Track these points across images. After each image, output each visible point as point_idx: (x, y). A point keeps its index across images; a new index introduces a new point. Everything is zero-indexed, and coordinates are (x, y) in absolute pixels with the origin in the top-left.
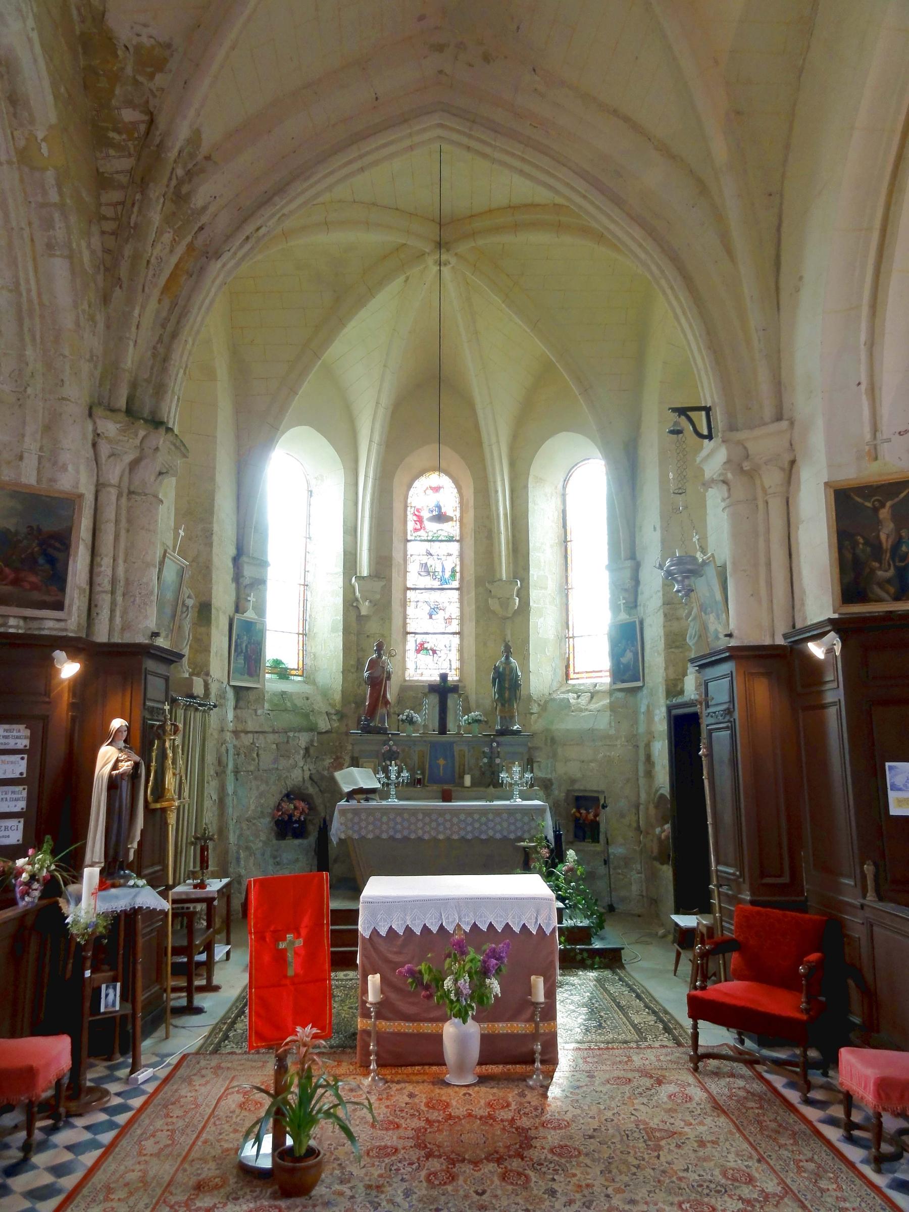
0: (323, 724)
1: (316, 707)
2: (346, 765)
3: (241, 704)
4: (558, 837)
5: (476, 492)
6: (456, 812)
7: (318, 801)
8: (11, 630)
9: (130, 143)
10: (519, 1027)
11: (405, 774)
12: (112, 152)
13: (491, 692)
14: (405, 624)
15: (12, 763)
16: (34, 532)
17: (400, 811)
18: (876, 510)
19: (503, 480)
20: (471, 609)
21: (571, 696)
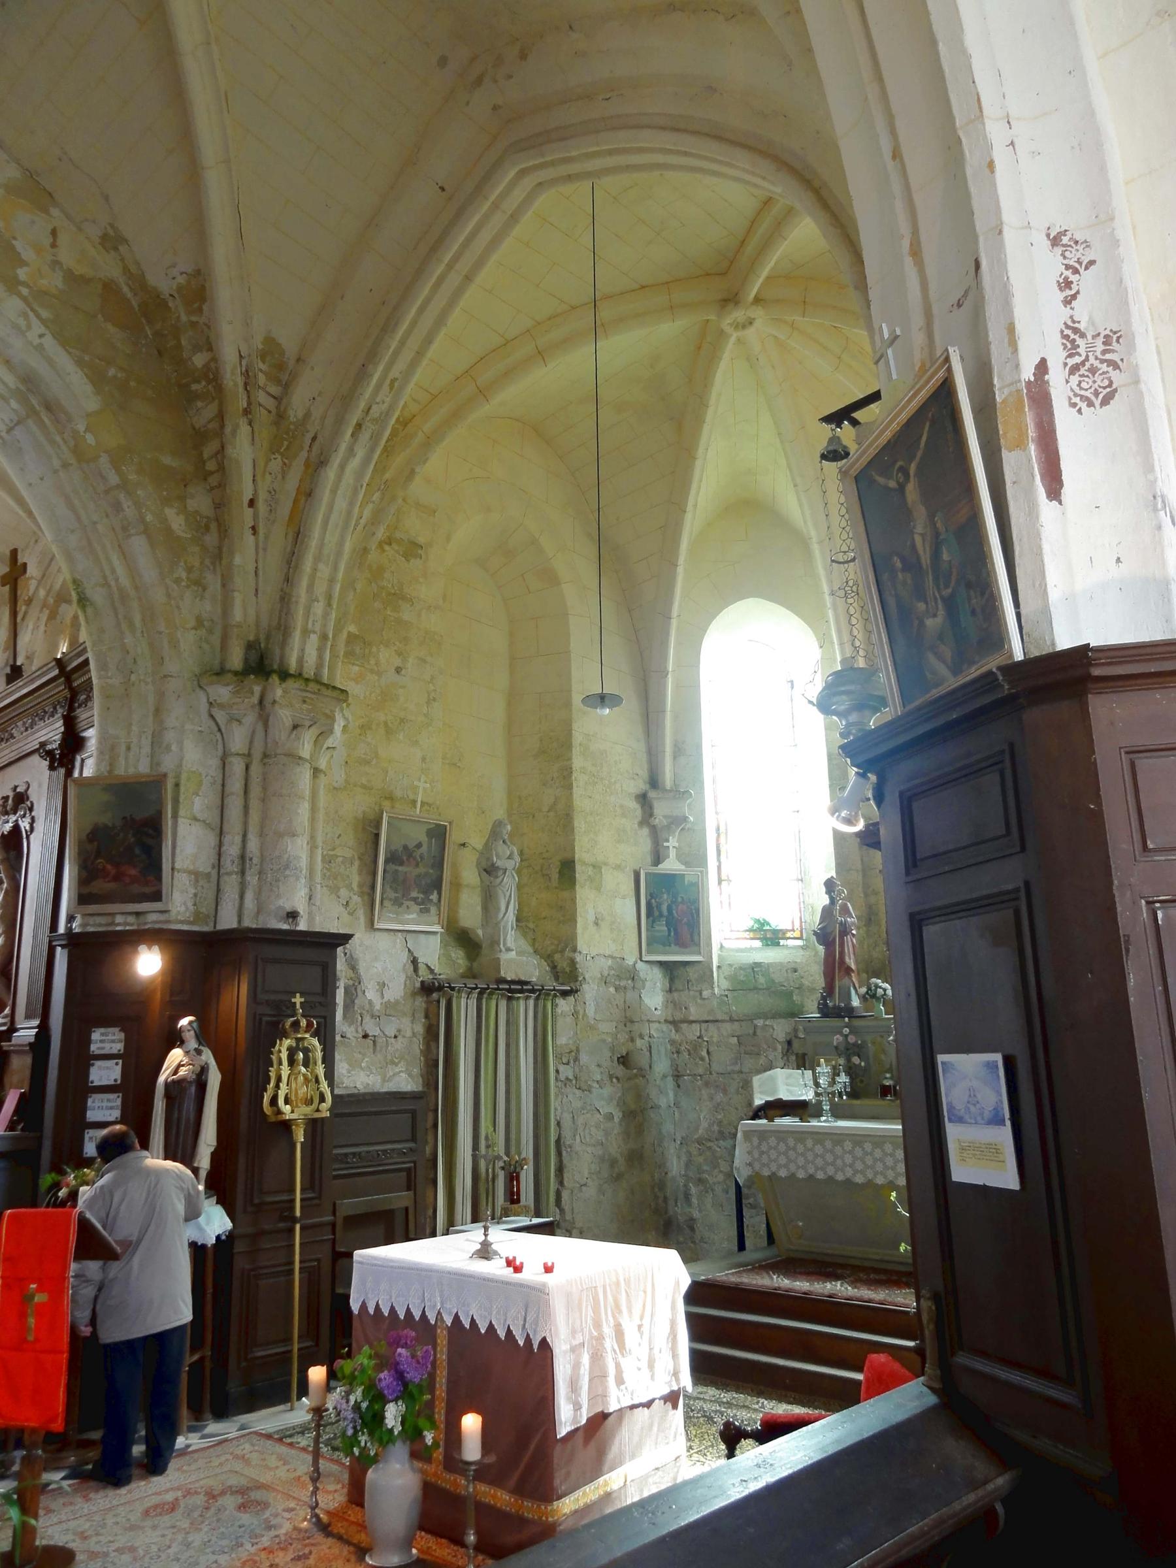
1: (806, 983)
3: (678, 984)
8: (118, 928)
9: (210, 386)
11: (843, 1078)
12: (199, 404)
15: (108, 1068)
16: (129, 823)
17: (838, 1138)
18: (902, 488)
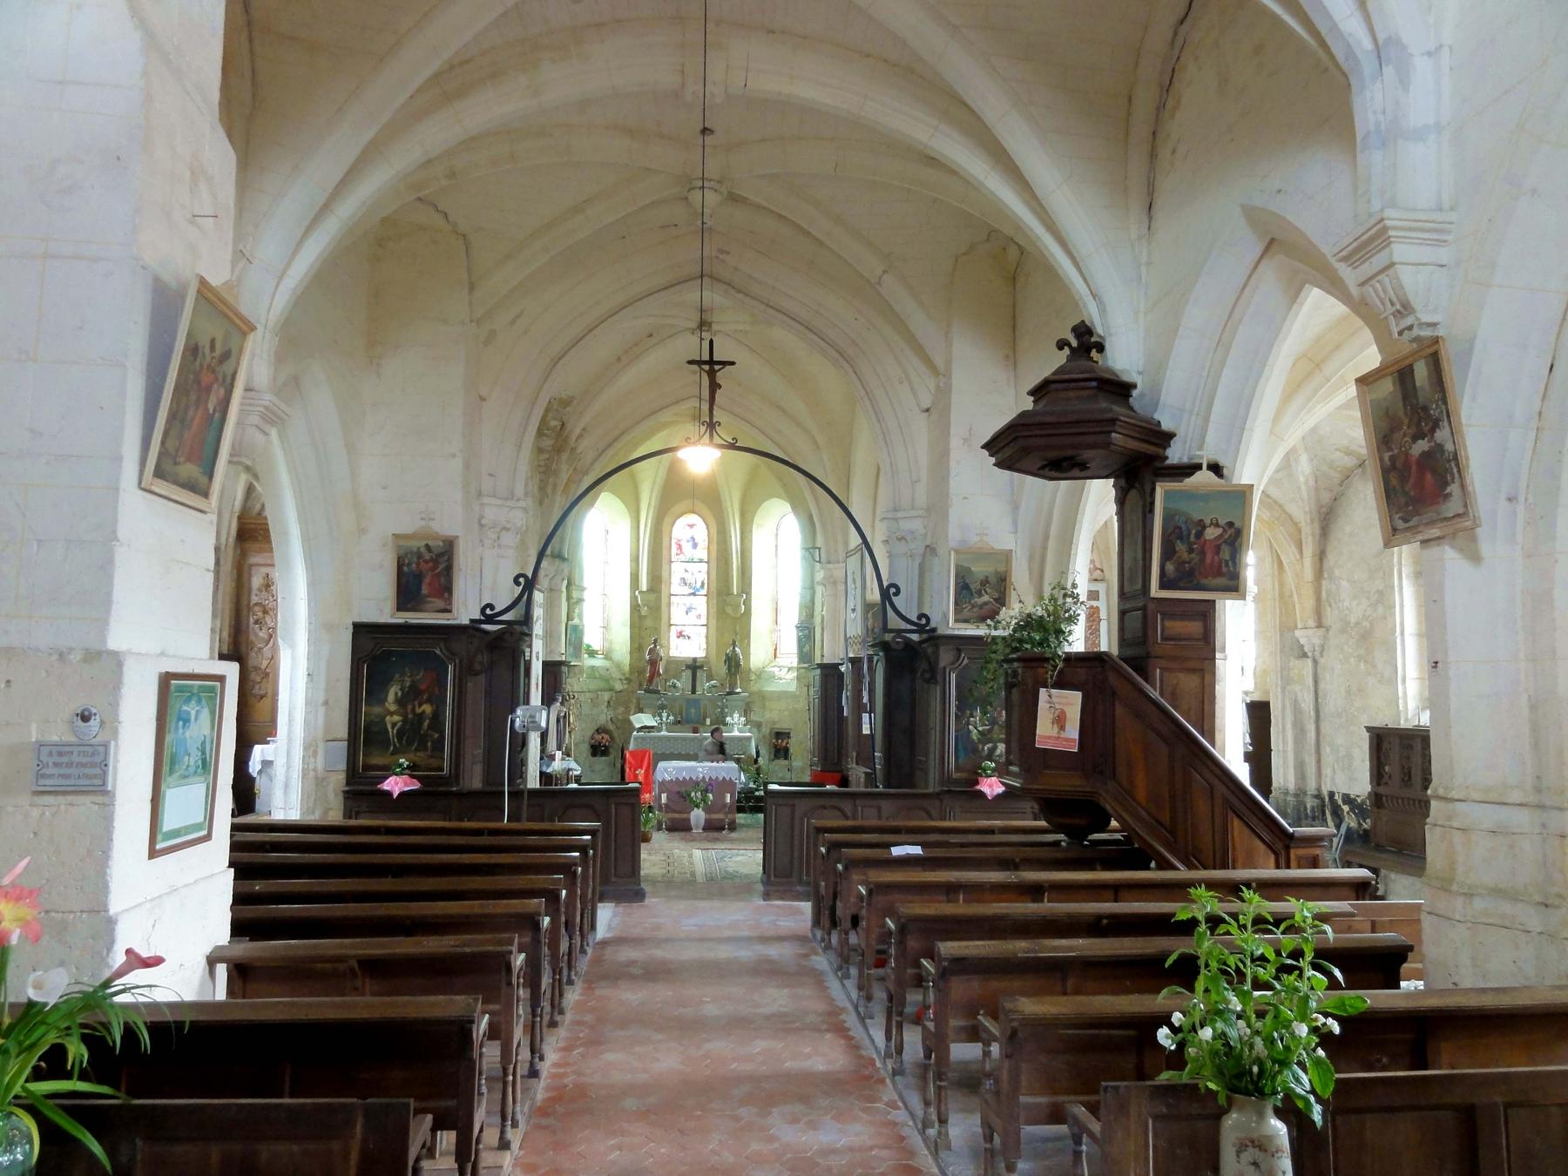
0: (618, 686)
1: (614, 676)
4: (758, 753)
5: (718, 532)
7: (616, 735)
10: (721, 816)
11: (671, 718)
13: (723, 670)
14: (669, 618)
19: (735, 529)
20: (713, 610)
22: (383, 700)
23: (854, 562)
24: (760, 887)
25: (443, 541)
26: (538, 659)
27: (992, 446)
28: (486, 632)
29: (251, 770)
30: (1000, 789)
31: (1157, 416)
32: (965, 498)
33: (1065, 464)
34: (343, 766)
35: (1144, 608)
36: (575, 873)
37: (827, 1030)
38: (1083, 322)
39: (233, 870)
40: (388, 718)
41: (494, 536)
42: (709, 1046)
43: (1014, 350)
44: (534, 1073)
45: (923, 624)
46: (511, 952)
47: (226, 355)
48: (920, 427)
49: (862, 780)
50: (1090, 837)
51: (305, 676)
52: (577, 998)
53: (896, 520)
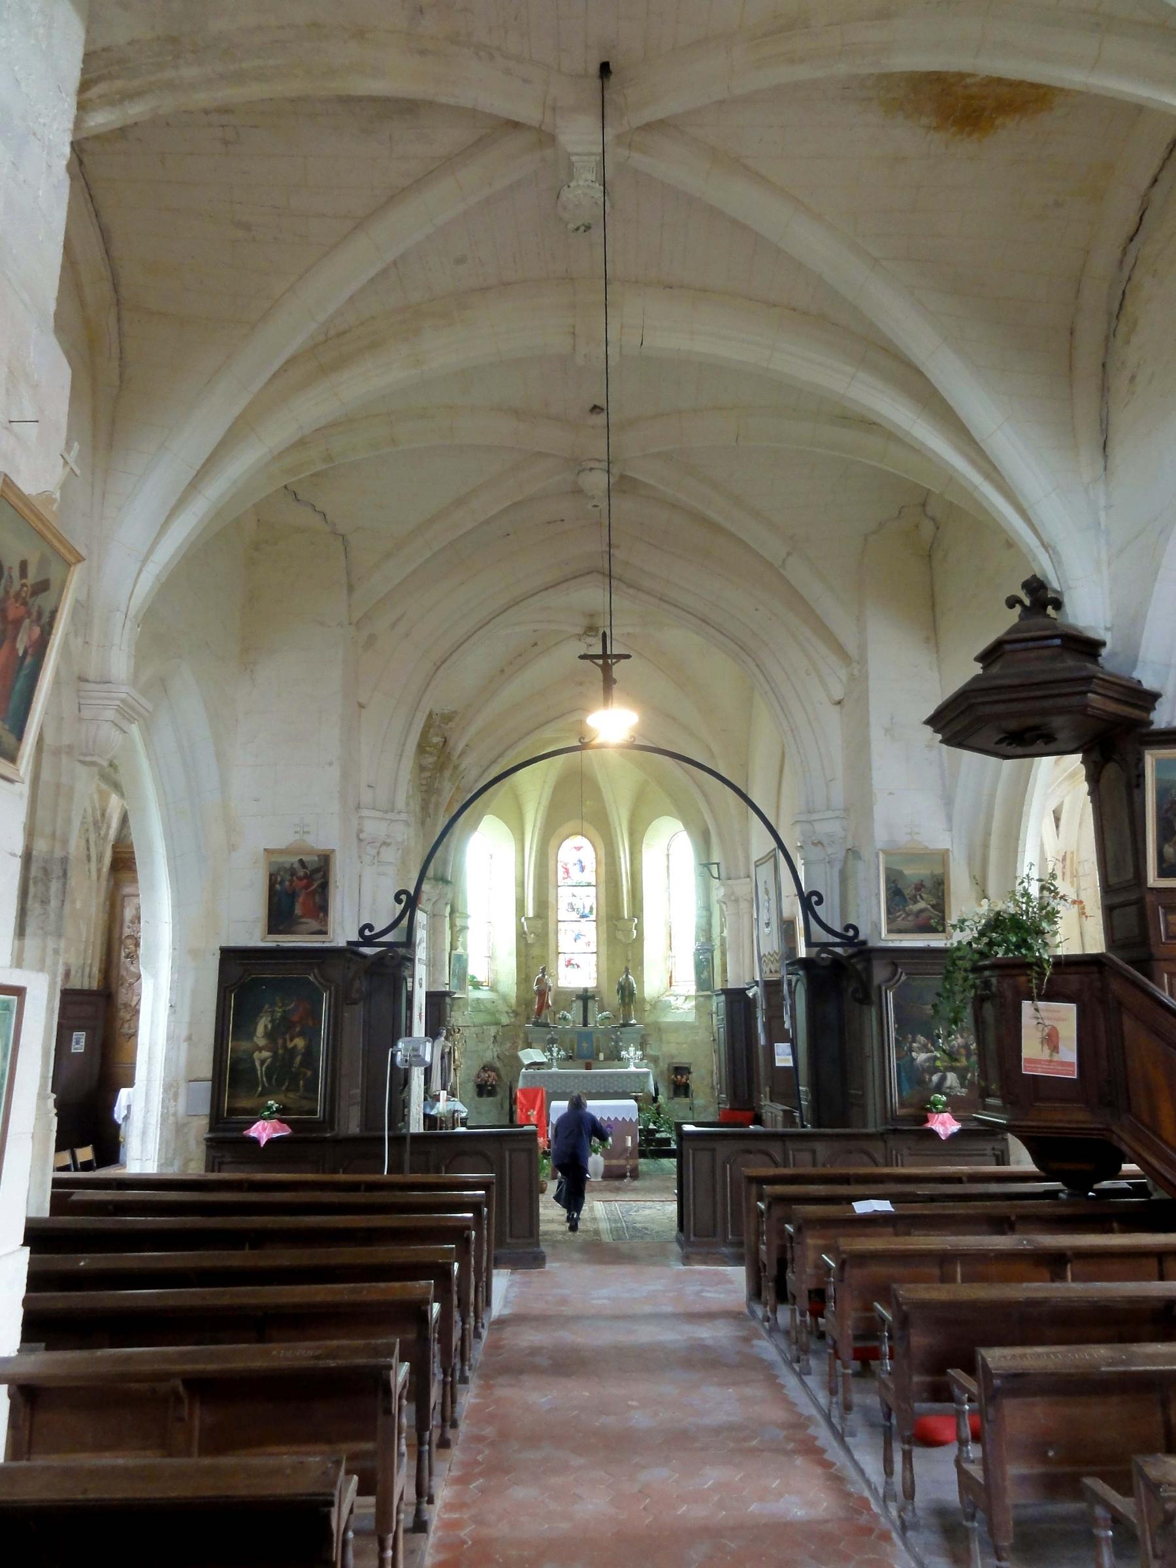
0: (505, 1020)
1: (499, 1008)
2: (519, 1047)
6: (595, 1076)
7: (503, 1072)
10: (622, 1162)
11: (562, 1053)
12: (427, 755)
13: (616, 999)
14: (557, 947)
19: (624, 849)
21: (672, 999)
22: (251, 1035)
23: (765, 872)
24: (676, 1248)
25: (318, 856)
26: (421, 986)
27: (937, 721)
28: (364, 956)
29: (116, 1116)
30: (955, 1127)
31: (1136, 675)
32: (891, 794)
33: (1028, 735)
34: (206, 1110)
35: (1140, 903)
36: (468, 1239)
37: (794, 1452)
38: (1034, 576)
39: (28, 1249)
40: (256, 1055)
41: (373, 852)
42: (644, 1476)
43: (936, 634)
44: (420, 1526)
45: (850, 937)
46: (390, 1367)
47: (42, 587)
48: (833, 724)
49: (780, 1119)
50: (1096, 1186)
51: (168, 1008)
52: (473, 1401)
53: (810, 822)
